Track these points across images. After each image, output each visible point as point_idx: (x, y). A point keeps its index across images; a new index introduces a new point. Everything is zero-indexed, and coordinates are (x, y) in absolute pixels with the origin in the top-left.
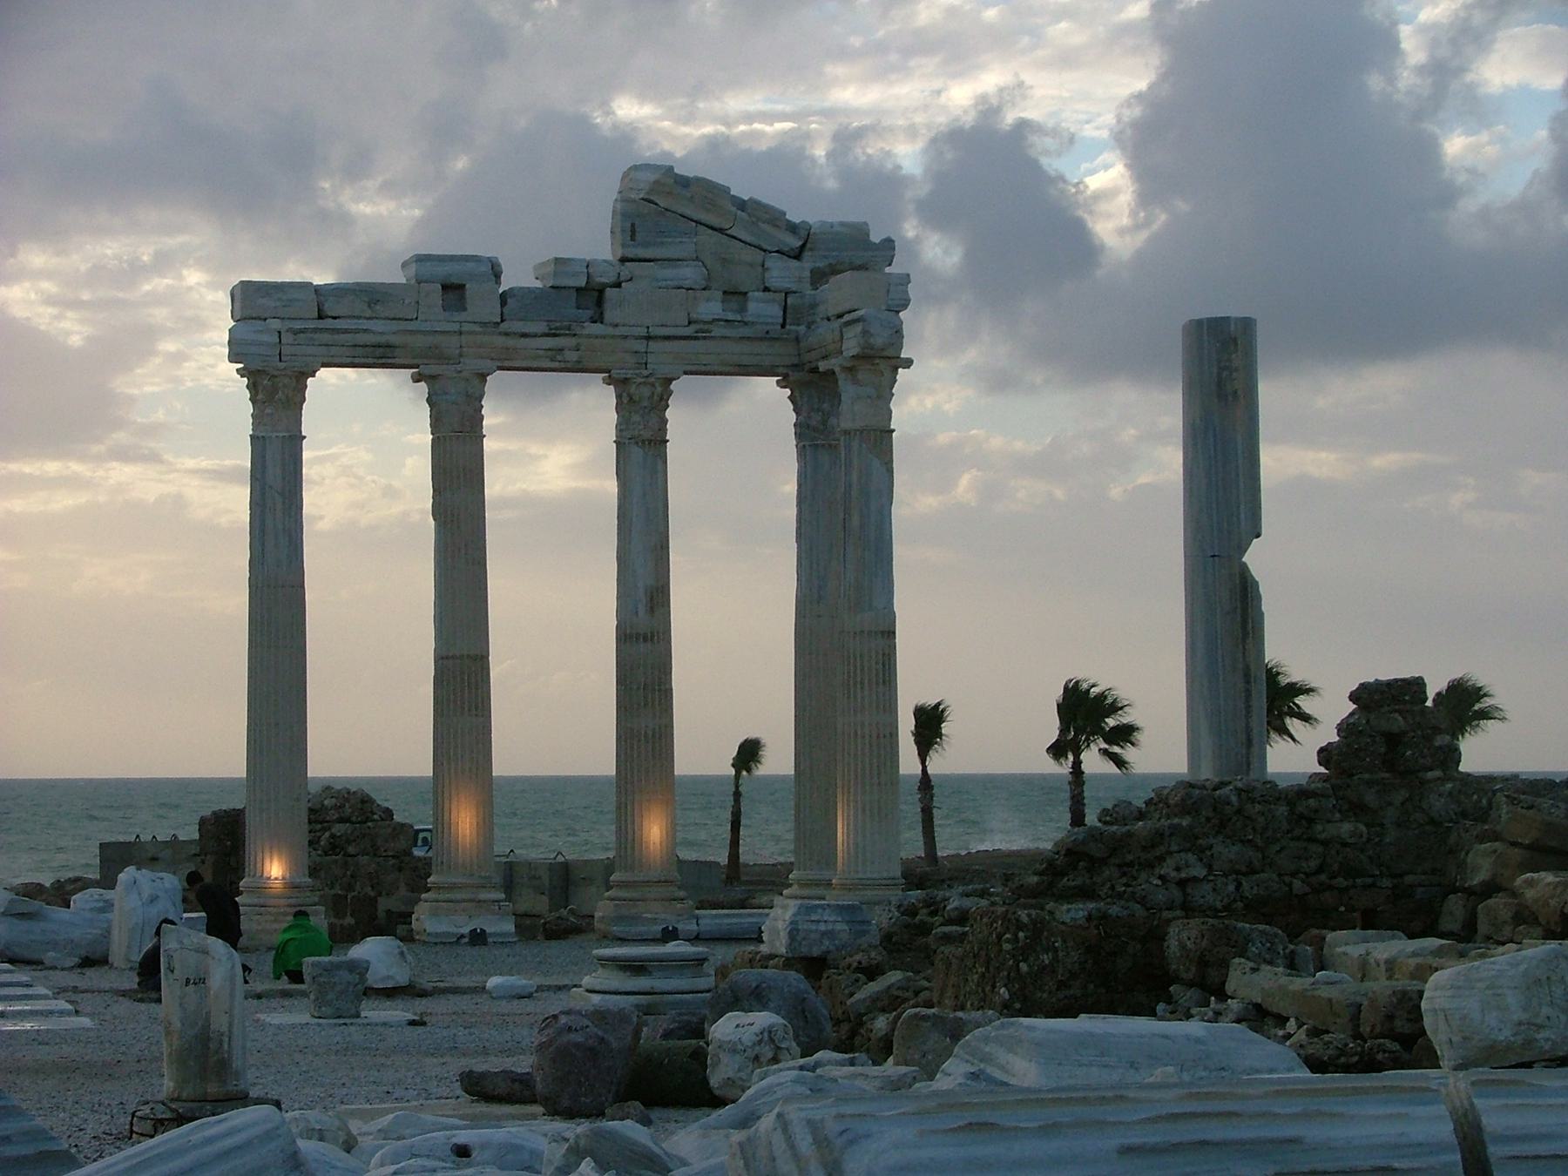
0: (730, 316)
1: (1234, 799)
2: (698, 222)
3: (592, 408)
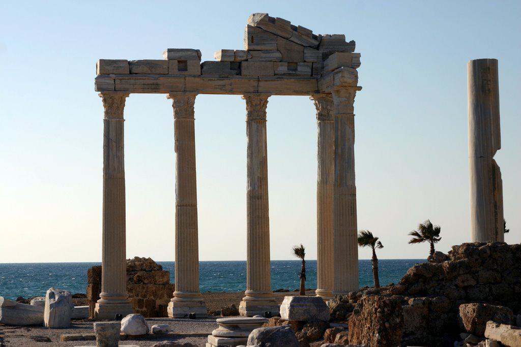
1: (488, 252)
3: (234, 107)
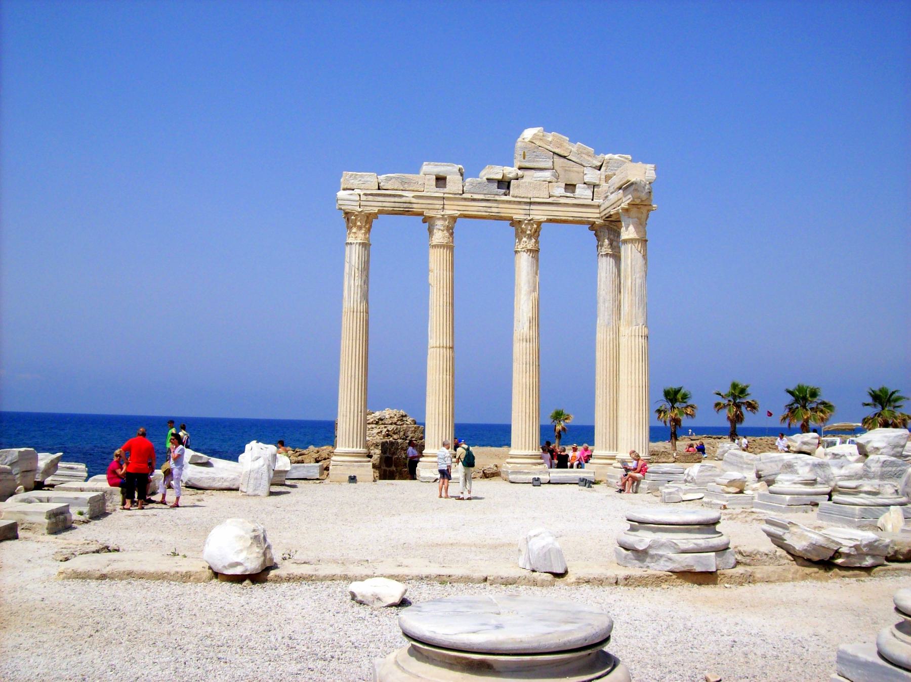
0: (568, 194)
2: (554, 153)
